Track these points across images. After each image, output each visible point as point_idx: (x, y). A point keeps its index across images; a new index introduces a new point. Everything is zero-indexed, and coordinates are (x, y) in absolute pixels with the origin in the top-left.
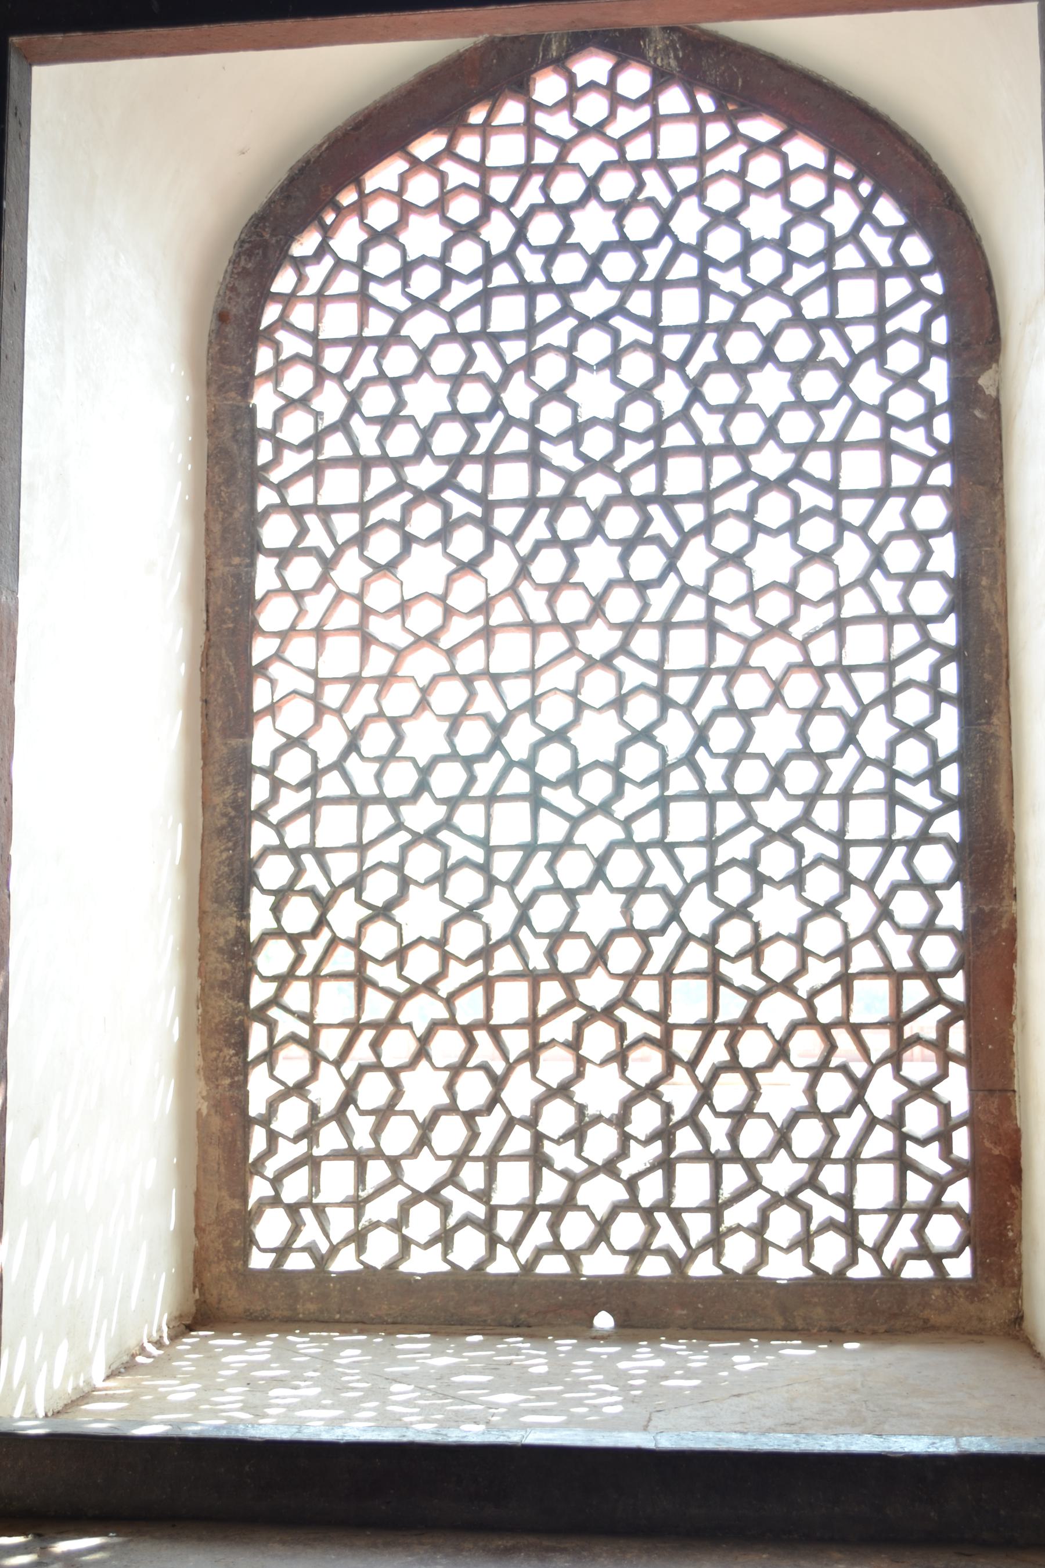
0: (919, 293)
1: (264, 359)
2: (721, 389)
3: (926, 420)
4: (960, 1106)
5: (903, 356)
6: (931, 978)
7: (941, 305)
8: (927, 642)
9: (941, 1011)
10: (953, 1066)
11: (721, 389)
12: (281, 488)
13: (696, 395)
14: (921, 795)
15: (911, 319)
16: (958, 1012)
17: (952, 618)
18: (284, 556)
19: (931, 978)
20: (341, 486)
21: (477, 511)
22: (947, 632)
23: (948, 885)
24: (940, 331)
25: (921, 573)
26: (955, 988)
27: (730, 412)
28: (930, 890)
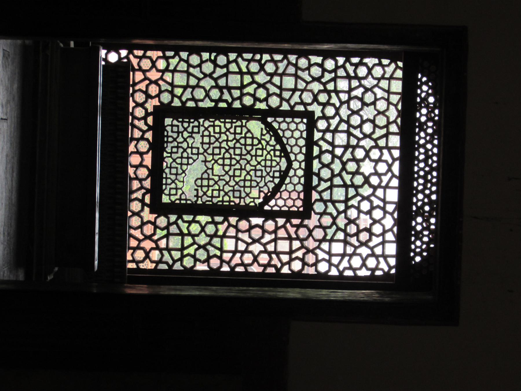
0: (390, 268)
1: (385, 62)
2: (365, 206)
3: (350, 268)
4: (142, 266)
5: (371, 263)
6: (181, 259)
7: (387, 275)
8: (283, 264)
9: (171, 262)
10: (154, 265)
11: (365, 206)
12: (343, 66)
13: (364, 198)
14: (237, 259)
15: (383, 265)
16: (170, 267)
17: (290, 272)
18: (321, 65)
19: (181, 259)
20: (343, 85)
21: (332, 128)
22: (285, 270)
23: (209, 266)
24: (378, 273)
25: (305, 264)
26: (177, 266)
27: (358, 208)
28: (207, 261)
